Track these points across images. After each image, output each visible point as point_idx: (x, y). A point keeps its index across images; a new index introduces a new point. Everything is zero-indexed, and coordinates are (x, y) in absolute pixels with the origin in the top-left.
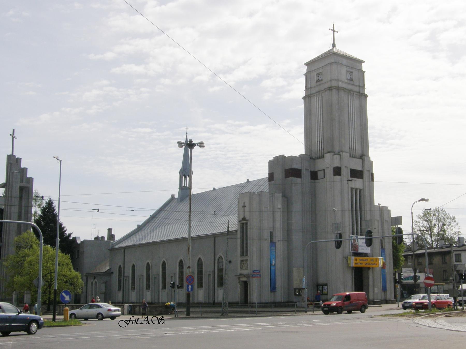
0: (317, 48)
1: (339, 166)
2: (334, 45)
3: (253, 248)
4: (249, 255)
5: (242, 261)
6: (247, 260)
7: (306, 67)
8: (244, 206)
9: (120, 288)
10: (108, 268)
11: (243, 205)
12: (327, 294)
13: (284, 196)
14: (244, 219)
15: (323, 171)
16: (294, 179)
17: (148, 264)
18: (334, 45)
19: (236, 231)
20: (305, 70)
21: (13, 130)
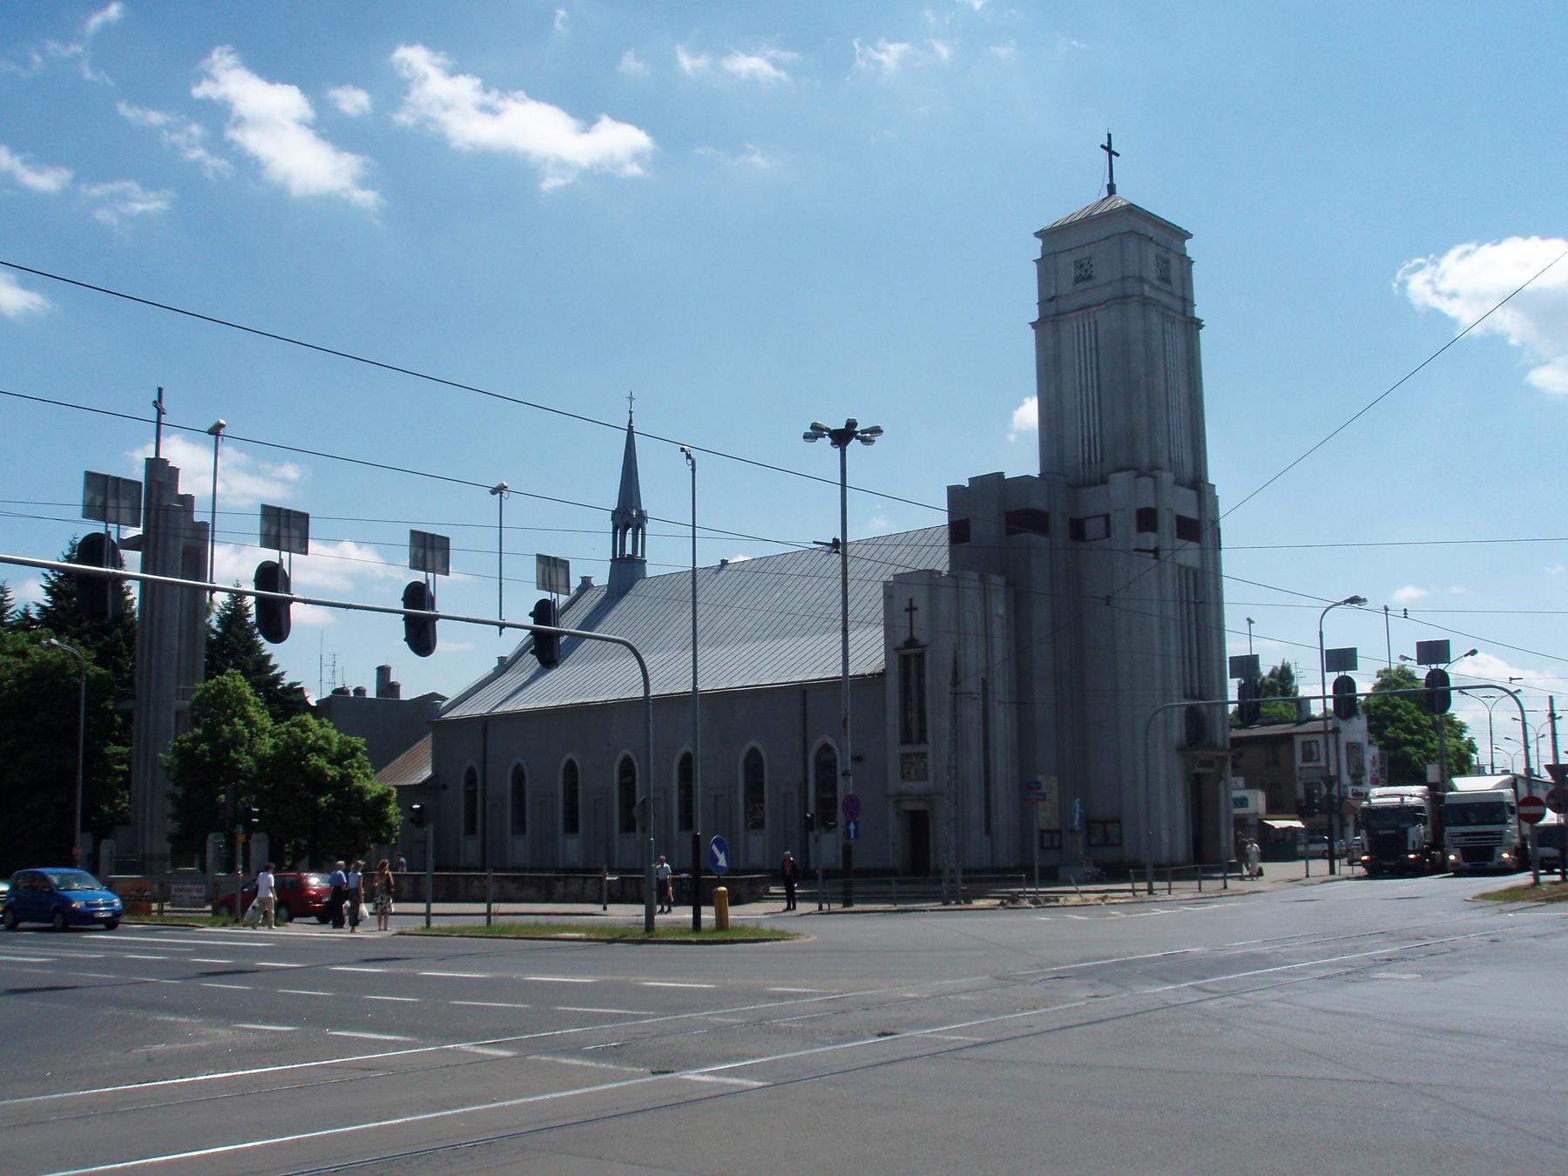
0: (1078, 196)
1: (1152, 505)
2: (1111, 189)
3: (939, 722)
4: (929, 739)
5: (905, 757)
6: (924, 755)
7: (1039, 242)
8: (911, 609)
9: (471, 830)
10: (427, 773)
11: (907, 605)
12: (1120, 845)
13: (1009, 584)
14: (911, 642)
15: (1102, 520)
16: (1034, 537)
17: (571, 768)
18: (1111, 189)
19: (882, 675)
20: (1036, 248)
21: (160, 390)
